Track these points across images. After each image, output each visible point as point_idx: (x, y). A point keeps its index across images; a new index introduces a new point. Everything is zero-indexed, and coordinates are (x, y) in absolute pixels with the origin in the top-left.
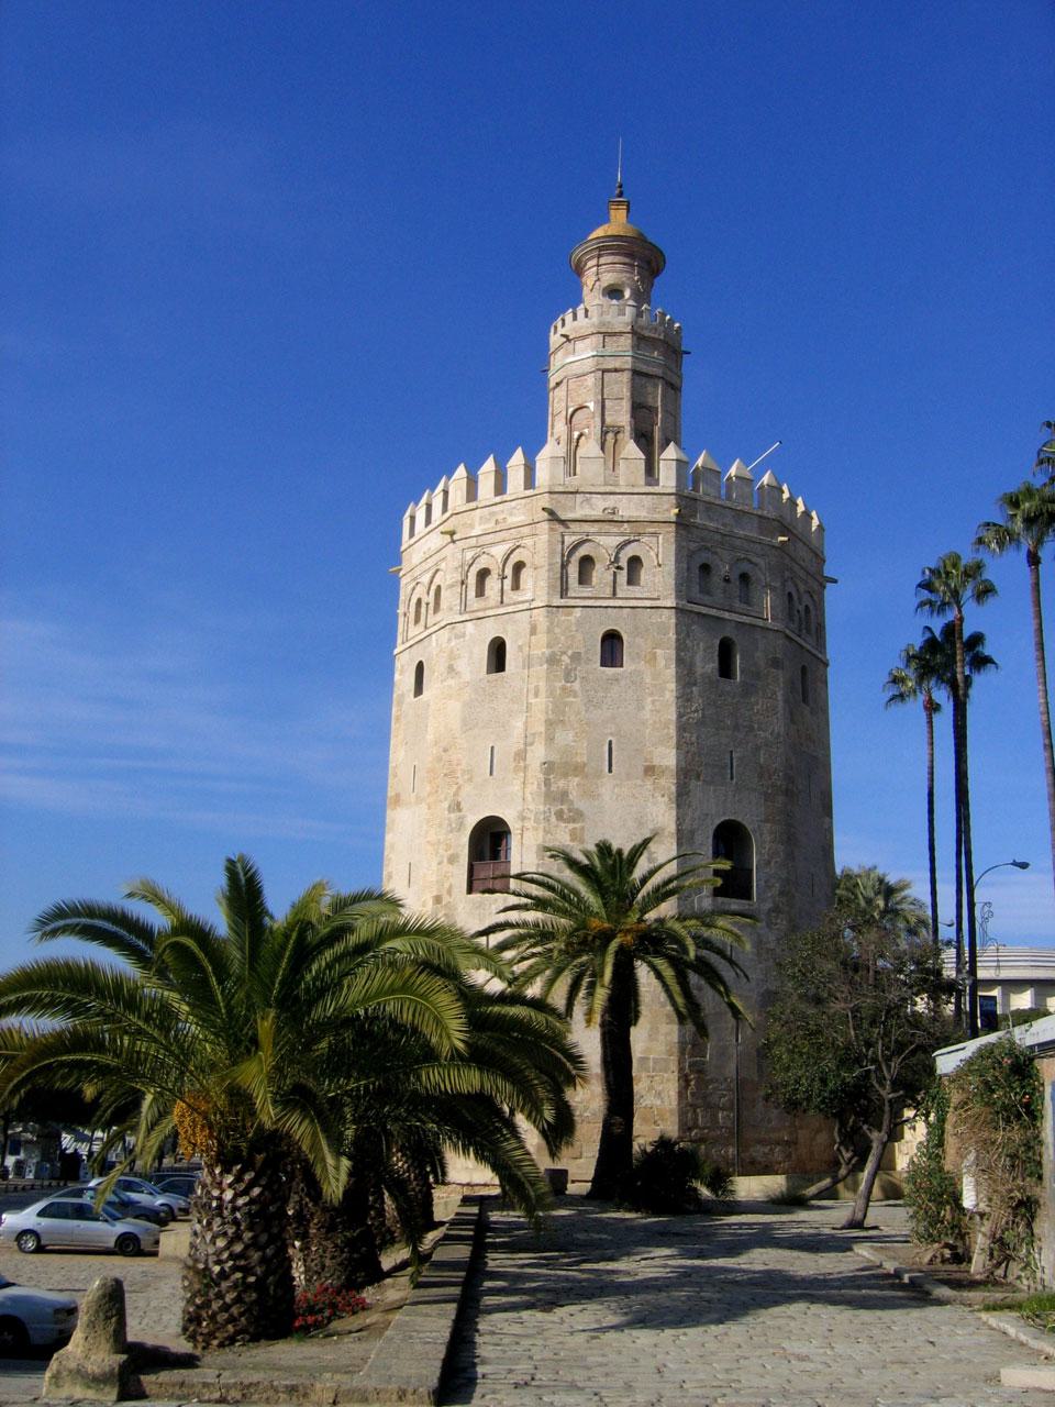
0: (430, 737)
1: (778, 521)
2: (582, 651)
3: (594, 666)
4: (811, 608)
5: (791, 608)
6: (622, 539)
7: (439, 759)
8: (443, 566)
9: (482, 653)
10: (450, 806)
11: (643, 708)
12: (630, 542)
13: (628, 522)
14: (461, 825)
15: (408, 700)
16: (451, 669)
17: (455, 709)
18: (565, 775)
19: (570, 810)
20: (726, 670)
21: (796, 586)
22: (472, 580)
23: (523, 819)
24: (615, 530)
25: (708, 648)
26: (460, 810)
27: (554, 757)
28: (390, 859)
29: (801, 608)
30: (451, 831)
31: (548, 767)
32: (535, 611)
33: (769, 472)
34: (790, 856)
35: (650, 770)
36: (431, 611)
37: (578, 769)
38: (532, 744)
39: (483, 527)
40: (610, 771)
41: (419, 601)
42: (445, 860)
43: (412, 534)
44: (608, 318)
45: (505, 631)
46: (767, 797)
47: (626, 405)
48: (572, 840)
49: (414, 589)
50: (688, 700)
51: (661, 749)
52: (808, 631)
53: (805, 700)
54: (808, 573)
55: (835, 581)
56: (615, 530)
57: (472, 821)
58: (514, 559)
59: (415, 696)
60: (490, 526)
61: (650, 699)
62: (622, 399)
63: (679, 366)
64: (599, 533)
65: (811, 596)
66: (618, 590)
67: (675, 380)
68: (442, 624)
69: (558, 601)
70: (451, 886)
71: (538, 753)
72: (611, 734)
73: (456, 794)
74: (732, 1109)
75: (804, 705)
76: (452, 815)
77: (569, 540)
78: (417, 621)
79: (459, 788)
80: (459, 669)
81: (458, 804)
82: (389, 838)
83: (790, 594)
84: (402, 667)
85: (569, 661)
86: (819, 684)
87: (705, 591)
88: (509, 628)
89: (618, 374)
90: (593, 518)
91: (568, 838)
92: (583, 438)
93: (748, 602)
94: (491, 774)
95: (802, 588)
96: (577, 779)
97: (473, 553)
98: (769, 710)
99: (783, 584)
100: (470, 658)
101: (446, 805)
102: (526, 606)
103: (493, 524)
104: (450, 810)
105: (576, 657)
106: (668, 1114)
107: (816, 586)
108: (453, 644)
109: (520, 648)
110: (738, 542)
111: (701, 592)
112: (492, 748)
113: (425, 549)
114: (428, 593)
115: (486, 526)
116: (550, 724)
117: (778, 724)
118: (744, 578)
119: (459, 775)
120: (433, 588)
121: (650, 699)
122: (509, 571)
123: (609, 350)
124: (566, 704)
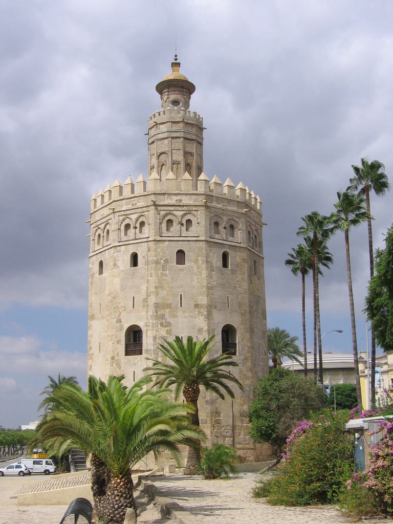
0: (107, 292)
1: (244, 203)
4: (257, 235)
5: (249, 237)
7: (112, 301)
9: (128, 259)
11: (193, 281)
13: (186, 206)
14: (121, 329)
15: (96, 276)
16: (115, 265)
17: (117, 281)
18: (164, 308)
19: (166, 322)
20: (225, 265)
21: (251, 228)
22: (123, 228)
23: (147, 326)
24: (181, 209)
25: (218, 256)
26: (121, 322)
27: (159, 301)
28: (90, 341)
29: (253, 237)
31: (157, 306)
32: (149, 243)
33: (240, 183)
34: (251, 337)
35: (196, 306)
36: (105, 240)
37: (169, 306)
39: (127, 207)
40: (181, 306)
41: (99, 235)
42: (116, 342)
43: (95, 207)
44: (173, 115)
46: (243, 315)
47: (182, 152)
48: (167, 334)
49: (97, 230)
50: (211, 277)
51: (201, 297)
52: (256, 246)
53: (255, 274)
54: (256, 222)
57: (126, 326)
60: (130, 207)
61: (196, 277)
62: (180, 150)
63: (202, 134)
64: (174, 210)
65: (257, 231)
66: (182, 233)
67: (200, 140)
68: (111, 246)
69: (159, 238)
70: (118, 353)
71: (153, 299)
72: (181, 292)
73: (119, 316)
74: (231, 437)
75: (254, 276)
77: (162, 213)
78: (99, 243)
79: (120, 313)
82: (90, 332)
83: (249, 232)
84: (93, 262)
86: (261, 267)
88: (139, 248)
90: (172, 204)
91: (165, 333)
92: (164, 166)
93: (233, 236)
94: (133, 308)
95: (254, 228)
96: (168, 310)
98: (241, 279)
99: (247, 228)
100: (123, 261)
101: (115, 320)
102: (145, 240)
104: (117, 322)
105: (166, 261)
107: (259, 227)
108: (116, 254)
110: (229, 213)
111: (215, 233)
112: (134, 297)
113: (101, 213)
114: (103, 232)
115: (129, 206)
116: (156, 287)
117: (245, 285)
120: (106, 230)
121: (196, 277)
122: (138, 225)
123: (174, 129)
124: (163, 280)
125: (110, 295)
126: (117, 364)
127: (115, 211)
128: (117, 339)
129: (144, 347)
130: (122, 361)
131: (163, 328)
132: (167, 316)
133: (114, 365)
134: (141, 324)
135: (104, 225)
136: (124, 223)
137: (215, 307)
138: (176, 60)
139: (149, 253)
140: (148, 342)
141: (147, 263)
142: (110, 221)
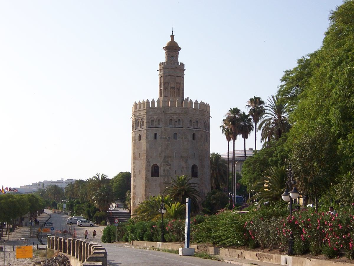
6: (176, 117)
8: (144, 117)
9: (153, 135)
14: (150, 166)
31: (165, 157)
35: (181, 157)
37: (170, 157)
55: (212, 117)
57: (152, 165)
58: (158, 119)
61: (181, 145)
77: (169, 116)
79: (149, 159)
81: (149, 162)
87: (191, 125)
89: (173, 77)
92: (167, 89)
105: (169, 138)
113: (140, 113)
118: (197, 121)
121: (181, 145)
129: (159, 174)
131: (167, 166)
132: (169, 161)
134: (158, 164)
136: (151, 120)
137: (189, 158)
138: (172, 33)
140: (161, 172)
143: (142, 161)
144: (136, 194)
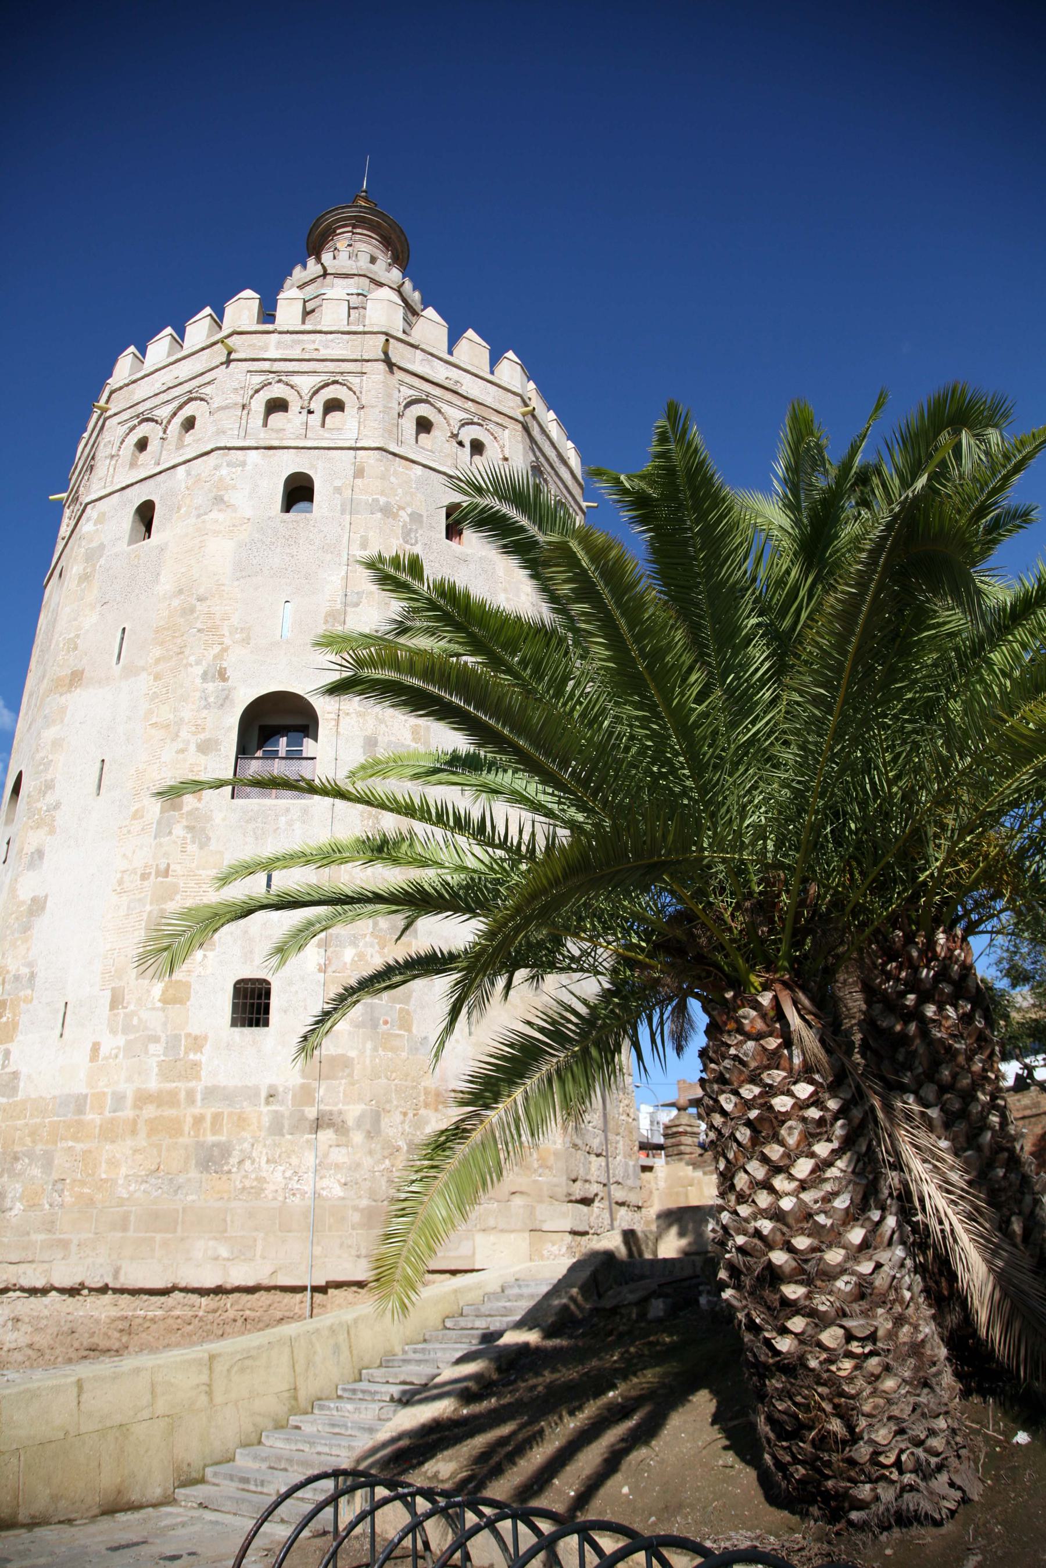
2: (425, 514)
3: (438, 536)
10: (205, 673)
12: (473, 423)
14: (225, 700)
24: (459, 401)
30: (205, 707)
38: (357, 605)
42: (193, 748)
45: (313, 466)
48: (414, 739)
56: (459, 403)
59: (129, 544)
73: (215, 657)
76: (211, 686)
79: (225, 650)
80: (233, 502)
81: (222, 675)
85: (407, 519)
97: (263, 378)
101: (199, 670)
103: (299, 351)
104: (205, 677)
106: (552, 1158)
109: (338, 490)
119: (227, 634)
125: (181, 592)
126: (190, 828)
127: (233, 356)
128: (202, 736)
130: (218, 818)
133: (179, 831)
135: (176, 404)
139: (358, 481)
141: (350, 507)
142: (208, 390)
143: (144, 682)
144: (32, 976)
